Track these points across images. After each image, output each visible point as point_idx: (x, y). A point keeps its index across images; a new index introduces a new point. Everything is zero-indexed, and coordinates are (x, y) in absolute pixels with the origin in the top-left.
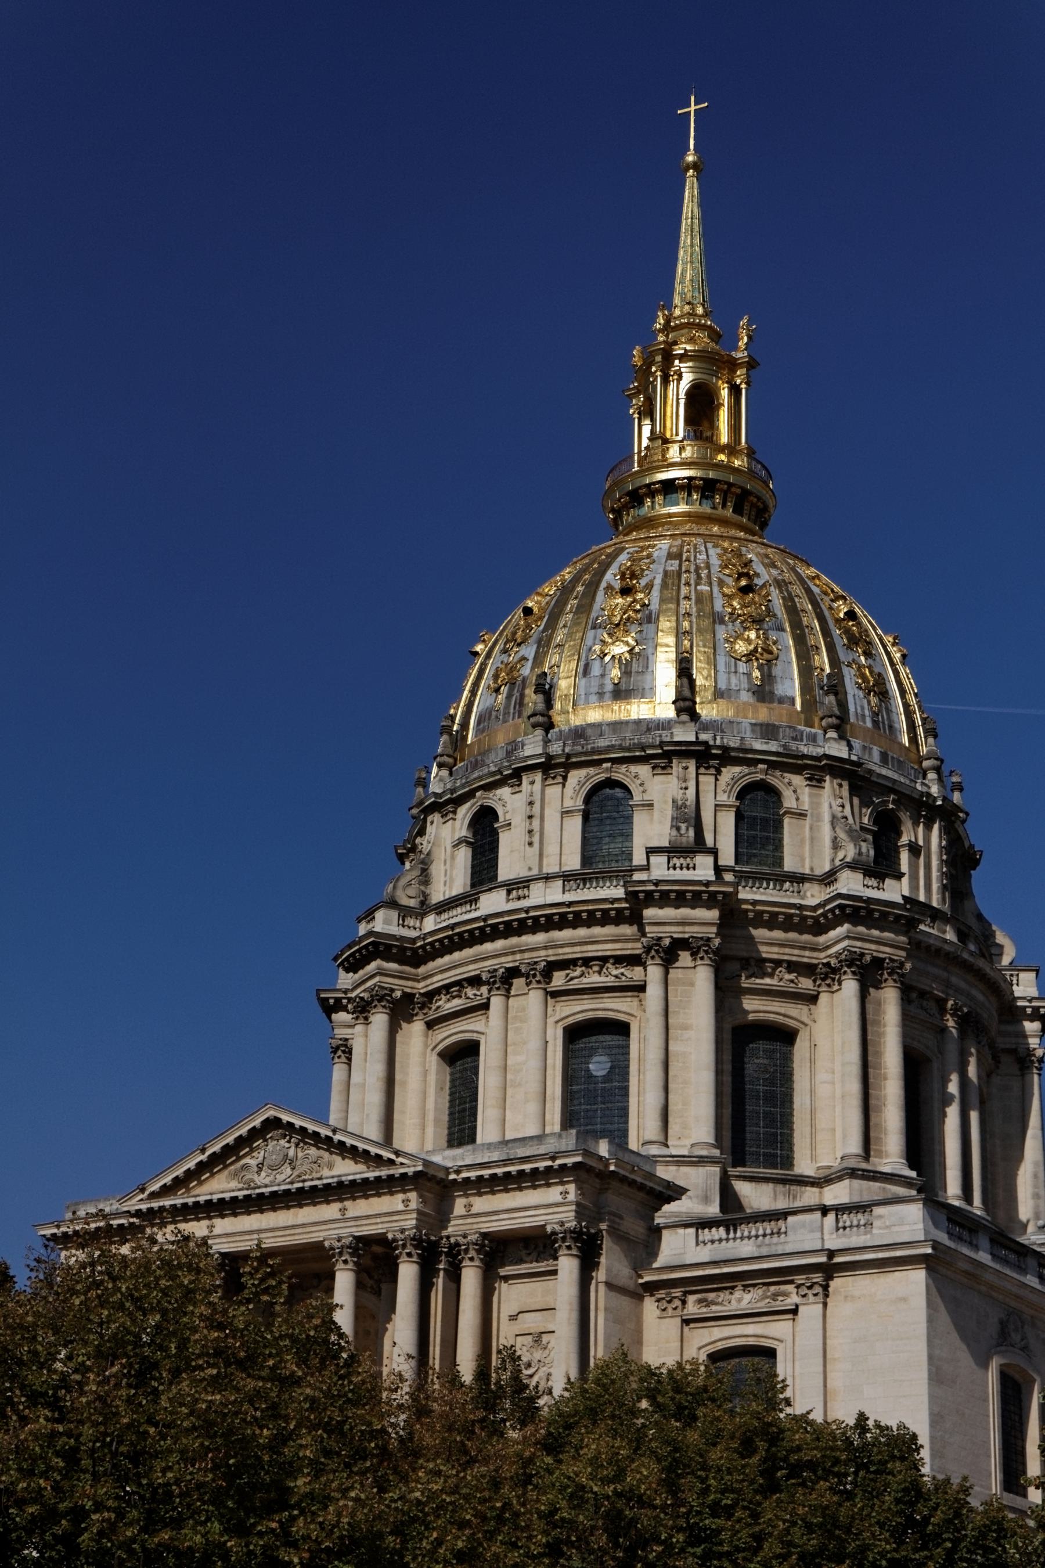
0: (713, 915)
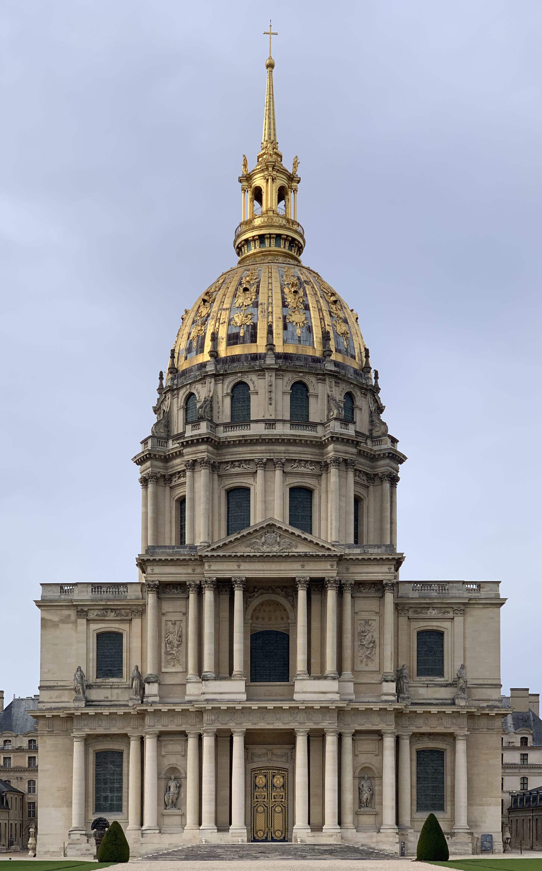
0: (354, 450)
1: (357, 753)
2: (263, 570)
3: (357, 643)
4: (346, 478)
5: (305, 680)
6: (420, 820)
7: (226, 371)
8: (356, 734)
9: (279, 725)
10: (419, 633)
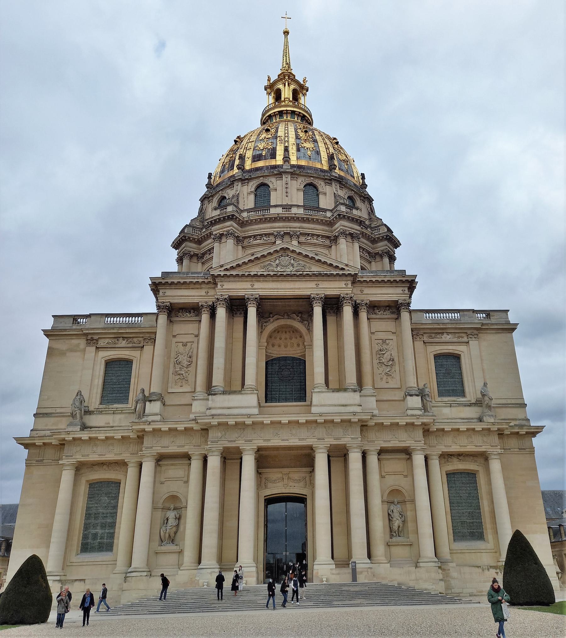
1: (383, 474)
2: (277, 289)
3: (376, 362)
4: (353, 248)
5: (323, 392)
6: (459, 551)
7: (250, 176)
8: (381, 452)
9: (294, 442)
10: (437, 357)
